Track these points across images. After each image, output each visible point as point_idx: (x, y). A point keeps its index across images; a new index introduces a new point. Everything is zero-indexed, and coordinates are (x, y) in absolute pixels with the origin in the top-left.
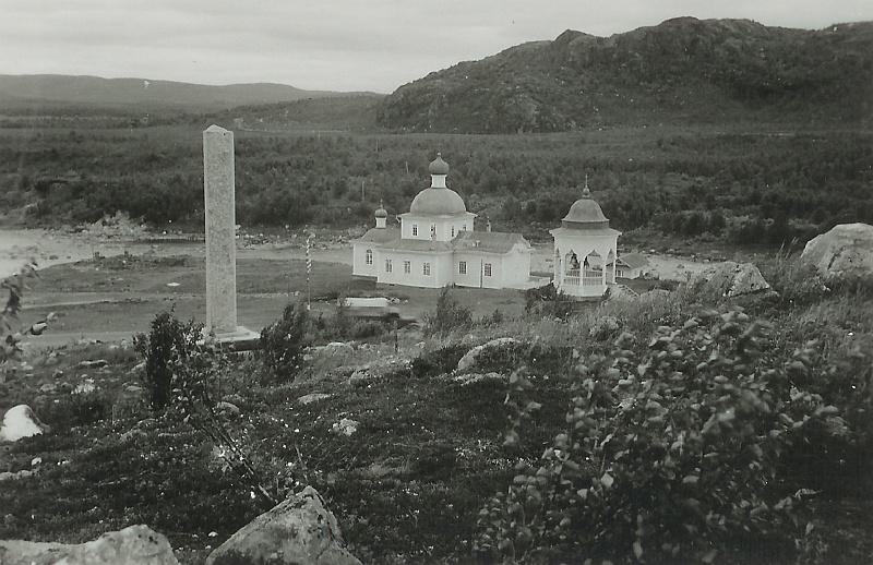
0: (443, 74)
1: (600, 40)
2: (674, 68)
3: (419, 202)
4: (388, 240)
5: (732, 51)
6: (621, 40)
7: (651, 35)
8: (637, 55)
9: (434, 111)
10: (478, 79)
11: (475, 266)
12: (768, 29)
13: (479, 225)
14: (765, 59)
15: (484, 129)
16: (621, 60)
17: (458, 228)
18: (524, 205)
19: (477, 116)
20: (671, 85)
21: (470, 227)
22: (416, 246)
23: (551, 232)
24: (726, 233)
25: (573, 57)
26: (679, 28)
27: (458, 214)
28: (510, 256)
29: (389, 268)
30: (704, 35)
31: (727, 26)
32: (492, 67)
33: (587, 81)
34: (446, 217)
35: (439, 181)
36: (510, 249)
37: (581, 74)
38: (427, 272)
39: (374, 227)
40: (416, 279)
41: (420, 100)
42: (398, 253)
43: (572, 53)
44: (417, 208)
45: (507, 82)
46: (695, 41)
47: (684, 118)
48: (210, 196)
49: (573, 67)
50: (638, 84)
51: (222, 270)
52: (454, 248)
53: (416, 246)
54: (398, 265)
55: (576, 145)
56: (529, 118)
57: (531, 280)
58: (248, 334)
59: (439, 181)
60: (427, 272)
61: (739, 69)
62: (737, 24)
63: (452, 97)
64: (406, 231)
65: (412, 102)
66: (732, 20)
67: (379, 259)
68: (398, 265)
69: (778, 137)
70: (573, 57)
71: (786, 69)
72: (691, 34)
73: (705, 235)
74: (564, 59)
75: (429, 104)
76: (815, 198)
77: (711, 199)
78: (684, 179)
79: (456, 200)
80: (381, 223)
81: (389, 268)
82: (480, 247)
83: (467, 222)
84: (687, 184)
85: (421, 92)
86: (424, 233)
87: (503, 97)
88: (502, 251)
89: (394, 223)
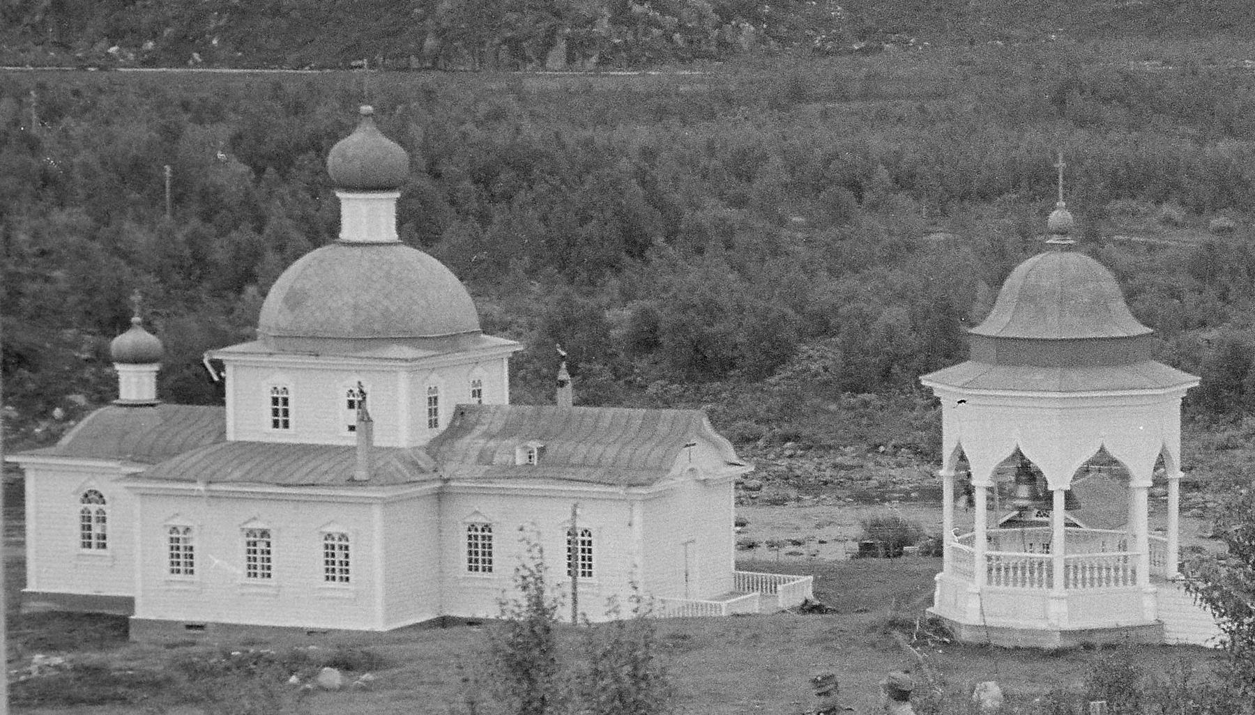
3: (294, 301)
4: (168, 454)
11: (529, 529)
13: (530, 378)
15: (419, 52)
18: (620, 319)
21: (497, 389)
22: (285, 467)
23: (925, 381)
27: (450, 341)
28: (661, 496)
29: (182, 557)
34: (408, 352)
35: (368, 217)
36: (661, 470)
38: (337, 562)
40: (298, 601)
42: (214, 497)
52: (431, 474)
53: (285, 467)
54: (221, 558)
55: (774, 104)
59: (368, 217)
60: (337, 562)
64: (245, 413)
68: (221, 558)
78: (1168, 221)
79: (434, 285)
80: (137, 383)
81: (182, 557)
82: (547, 466)
84: (1187, 242)
86: (321, 417)
88: (635, 477)
89: (193, 386)
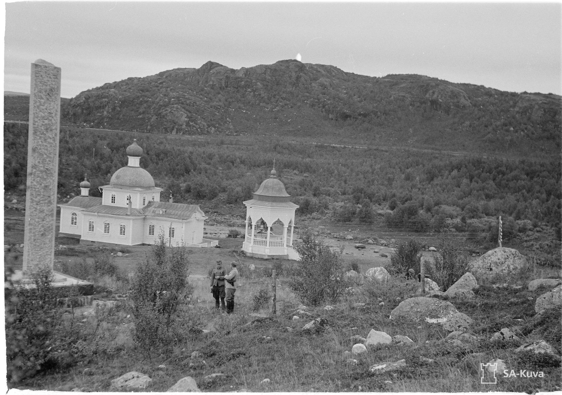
0: (116, 85)
1: (233, 71)
2: (284, 95)
3: (118, 177)
4: (90, 207)
5: (324, 86)
6: (248, 72)
7: (269, 70)
8: (258, 83)
9: (108, 112)
10: (142, 91)
11: (162, 227)
12: (347, 73)
13: (164, 196)
14: (346, 93)
15: (146, 129)
16: (247, 86)
17: (148, 198)
18: (183, 186)
19: (141, 119)
20: (282, 106)
21: (157, 198)
22: (113, 211)
23: (244, 203)
24: (330, 213)
25: (213, 82)
26: (288, 67)
27: (149, 188)
28: (189, 222)
29: (91, 228)
30: (305, 74)
31: (319, 69)
32: (153, 84)
33: (223, 99)
34: (140, 189)
35: (134, 162)
36: (189, 217)
37: (219, 93)
38: (123, 231)
39: (78, 195)
40: (114, 238)
41: (97, 103)
42: (99, 216)
43: (212, 78)
44: (116, 181)
45: (165, 95)
46: (298, 78)
47: (290, 131)
48: (35, 133)
49: (212, 88)
50: (259, 104)
51: (42, 211)
52: (143, 215)
53: (113, 211)
54: (99, 228)
55: (217, 145)
56: (180, 123)
57: (204, 242)
58: (65, 280)
59: (134, 162)
60: (123, 231)
61: (329, 100)
62: (326, 68)
63: (124, 103)
64: (106, 199)
65: (91, 104)
66: (323, 66)
67: (84, 220)
68: (99, 228)
69: (356, 148)
70: (213, 82)
71: (360, 102)
72: (296, 72)
73: (314, 214)
74: (207, 82)
75: (104, 107)
76: (388, 193)
77: (316, 189)
78: (295, 174)
79: (146, 176)
80: (85, 192)
81: (91, 228)
82: (166, 214)
83: (156, 195)
84: (299, 178)
85: (99, 97)
86: (121, 201)
87: (162, 106)
88: (184, 218)
89: (96, 193)
